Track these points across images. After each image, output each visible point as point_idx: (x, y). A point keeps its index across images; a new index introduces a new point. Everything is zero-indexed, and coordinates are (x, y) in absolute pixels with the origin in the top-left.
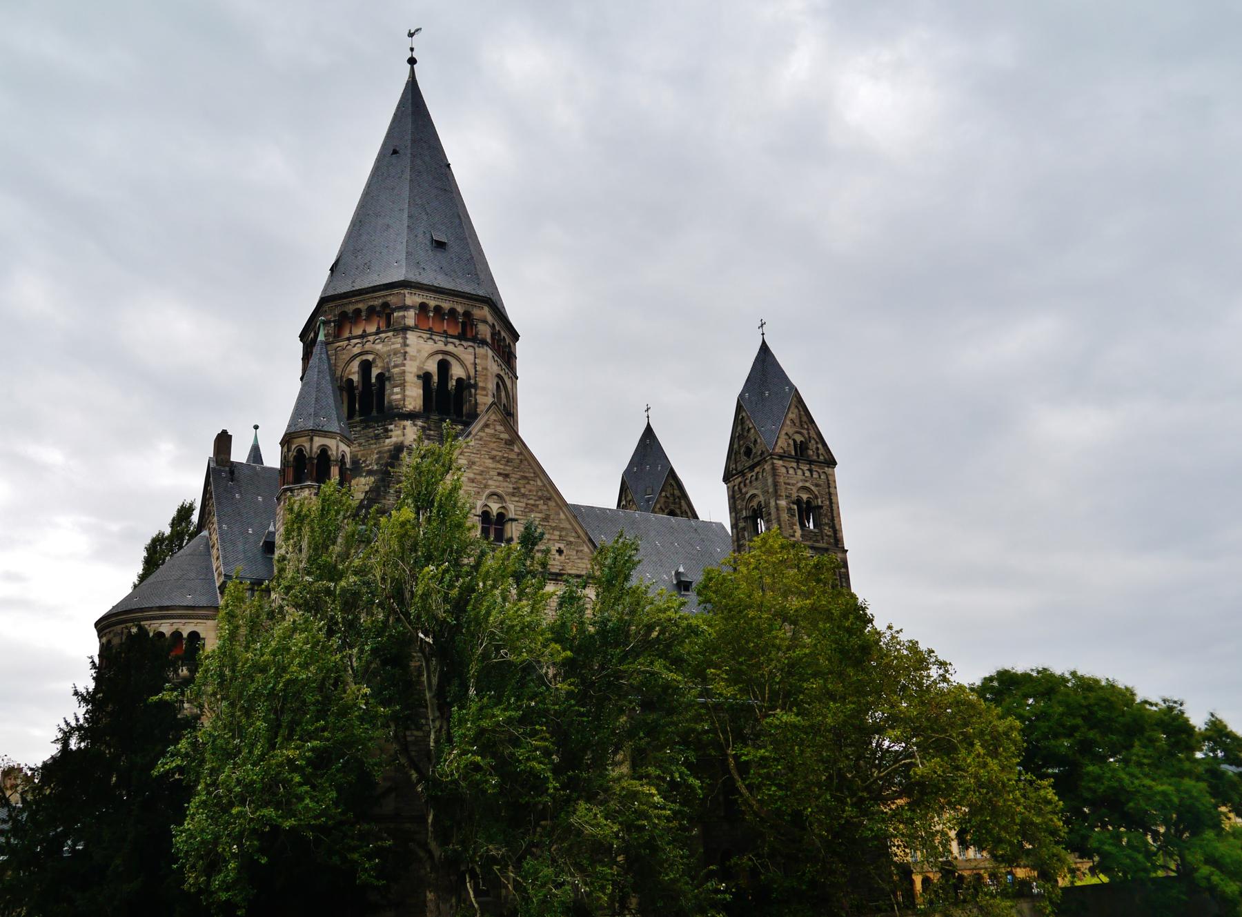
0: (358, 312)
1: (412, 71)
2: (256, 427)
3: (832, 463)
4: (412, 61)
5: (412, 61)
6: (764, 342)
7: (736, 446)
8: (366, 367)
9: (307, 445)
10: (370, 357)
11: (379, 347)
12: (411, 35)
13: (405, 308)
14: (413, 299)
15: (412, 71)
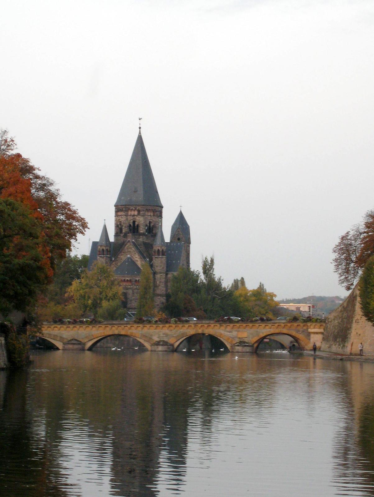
0: (150, 209)
1: (140, 130)
2: (105, 220)
3: (190, 243)
4: (140, 128)
5: (140, 128)
6: (181, 211)
7: (175, 236)
8: (150, 223)
9: (164, 249)
10: (151, 221)
11: (154, 219)
12: (140, 119)
13: (158, 212)
14: (160, 209)
15: (140, 130)
